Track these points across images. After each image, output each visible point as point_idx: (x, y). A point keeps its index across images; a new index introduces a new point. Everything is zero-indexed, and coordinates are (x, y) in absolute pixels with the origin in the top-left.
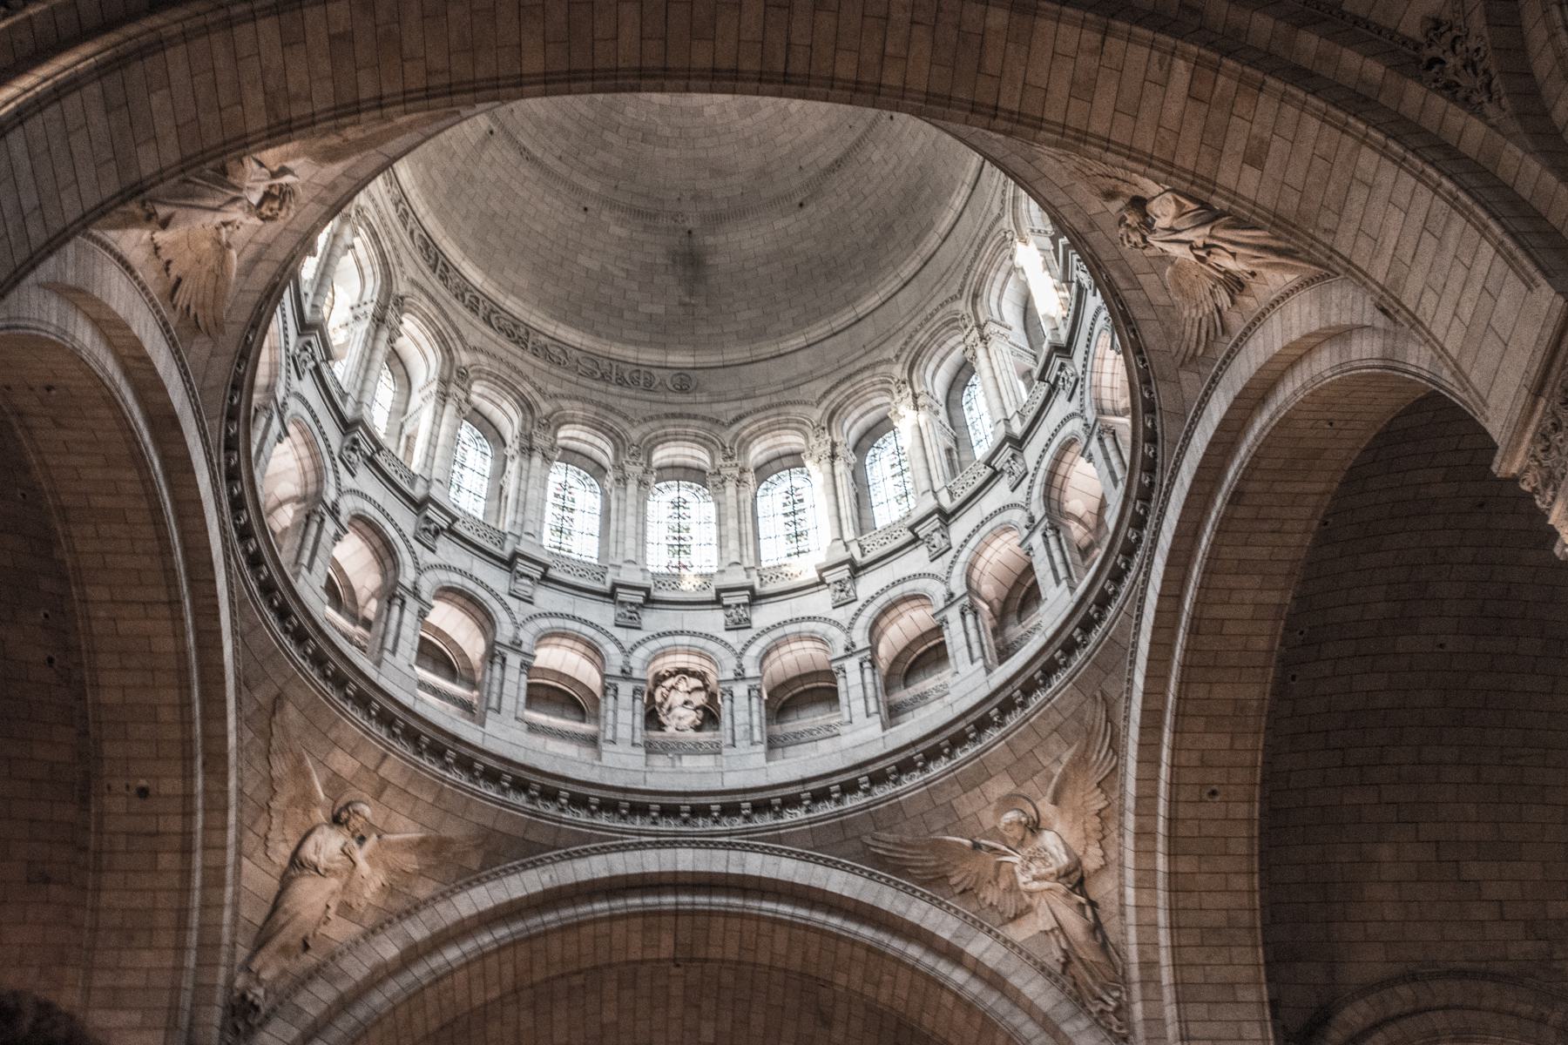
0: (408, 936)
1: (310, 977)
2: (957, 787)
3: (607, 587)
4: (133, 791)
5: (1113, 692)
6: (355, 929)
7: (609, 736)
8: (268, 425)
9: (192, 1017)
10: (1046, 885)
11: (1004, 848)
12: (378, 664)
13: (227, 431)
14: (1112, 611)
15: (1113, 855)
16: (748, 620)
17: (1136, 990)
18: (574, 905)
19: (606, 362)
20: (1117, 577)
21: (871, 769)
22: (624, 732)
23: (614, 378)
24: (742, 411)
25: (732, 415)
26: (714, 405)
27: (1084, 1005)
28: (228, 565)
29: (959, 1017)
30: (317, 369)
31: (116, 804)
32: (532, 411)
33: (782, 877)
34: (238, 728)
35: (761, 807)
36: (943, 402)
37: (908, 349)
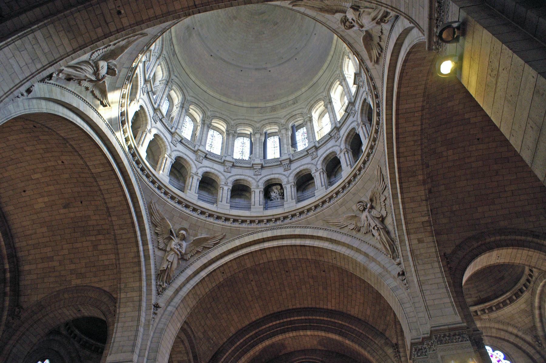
2: (179, 215)
5: (226, 237)
10: (178, 253)
11: (175, 235)
15: (192, 260)
27: (157, 280)
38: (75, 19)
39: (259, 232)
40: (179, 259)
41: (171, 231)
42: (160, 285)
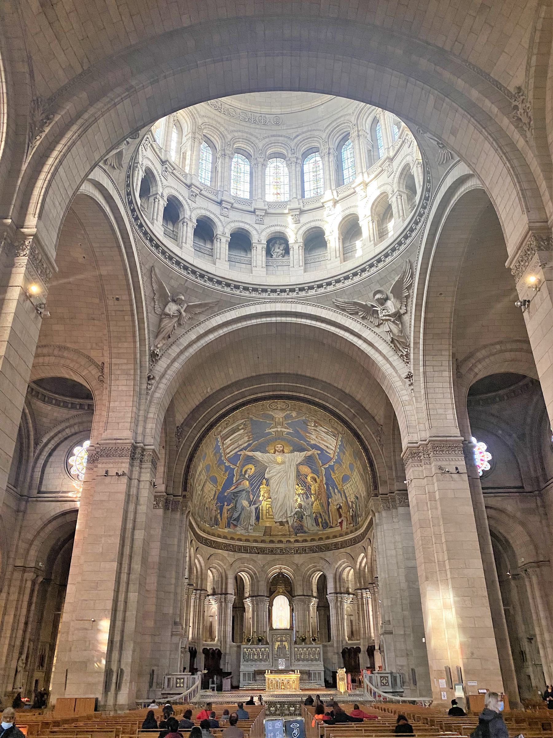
0: (198, 332)
1: (172, 345)
2: (362, 286)
3: (252, 210)
4: (115, 299)
5: (412, 261)
6: (183, 331)
7: (255, 265)
8: (138, 173)
9: (140, 359)
10: (387, 318)
12: (181, 248)
13: (127, 191)
14: (414, 234)
15: (409, 309)
16: (299, 220)
17: (412, 349)
18: (246, 321)
19: (250, 113)
20: (417, 223)
21: (336, 278)
22: (259, 263)
23: (253, 120)
24: (298, 133)
25: (294, 135)
26: (288, 130)
28: (133, 231)
29: (360, 354)
30: (151, 145)
31: (110, 303)
32: (225, 139)
33: (307, 312)
34: (142, 277)
35: (302, 289)
36: (368, 131)
37: (357, 110)
38: (113, 331)
39: (424, 230)
40: (393, 322)
41: (372, 305)
42: (402, 355)
